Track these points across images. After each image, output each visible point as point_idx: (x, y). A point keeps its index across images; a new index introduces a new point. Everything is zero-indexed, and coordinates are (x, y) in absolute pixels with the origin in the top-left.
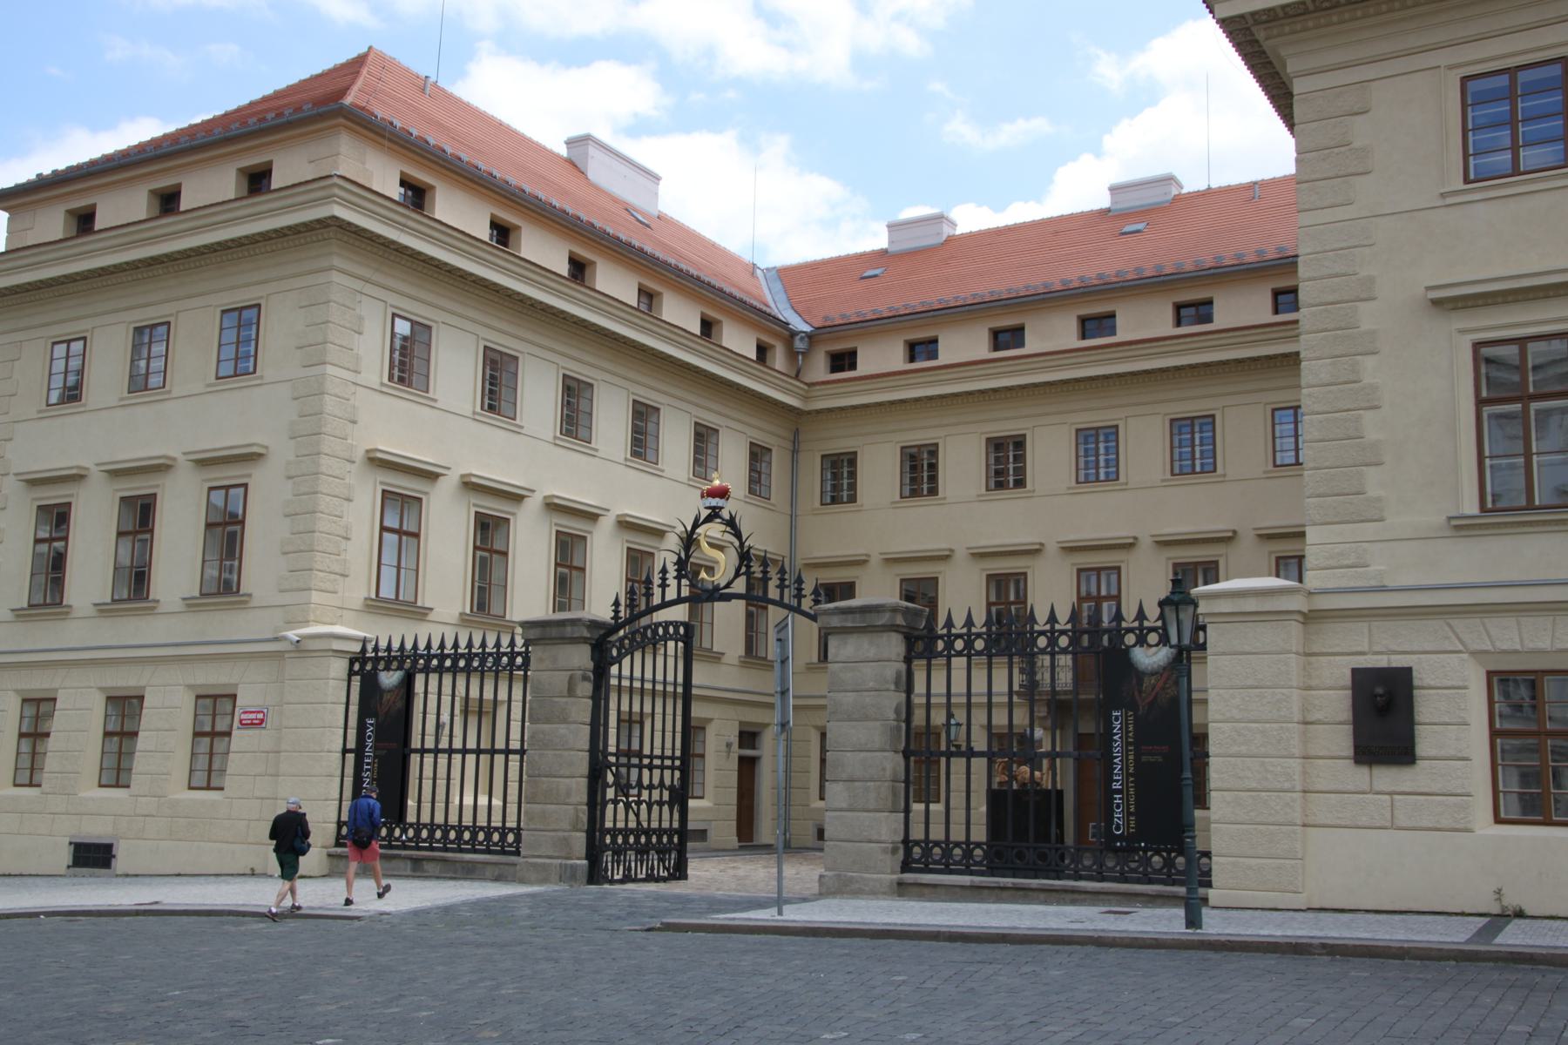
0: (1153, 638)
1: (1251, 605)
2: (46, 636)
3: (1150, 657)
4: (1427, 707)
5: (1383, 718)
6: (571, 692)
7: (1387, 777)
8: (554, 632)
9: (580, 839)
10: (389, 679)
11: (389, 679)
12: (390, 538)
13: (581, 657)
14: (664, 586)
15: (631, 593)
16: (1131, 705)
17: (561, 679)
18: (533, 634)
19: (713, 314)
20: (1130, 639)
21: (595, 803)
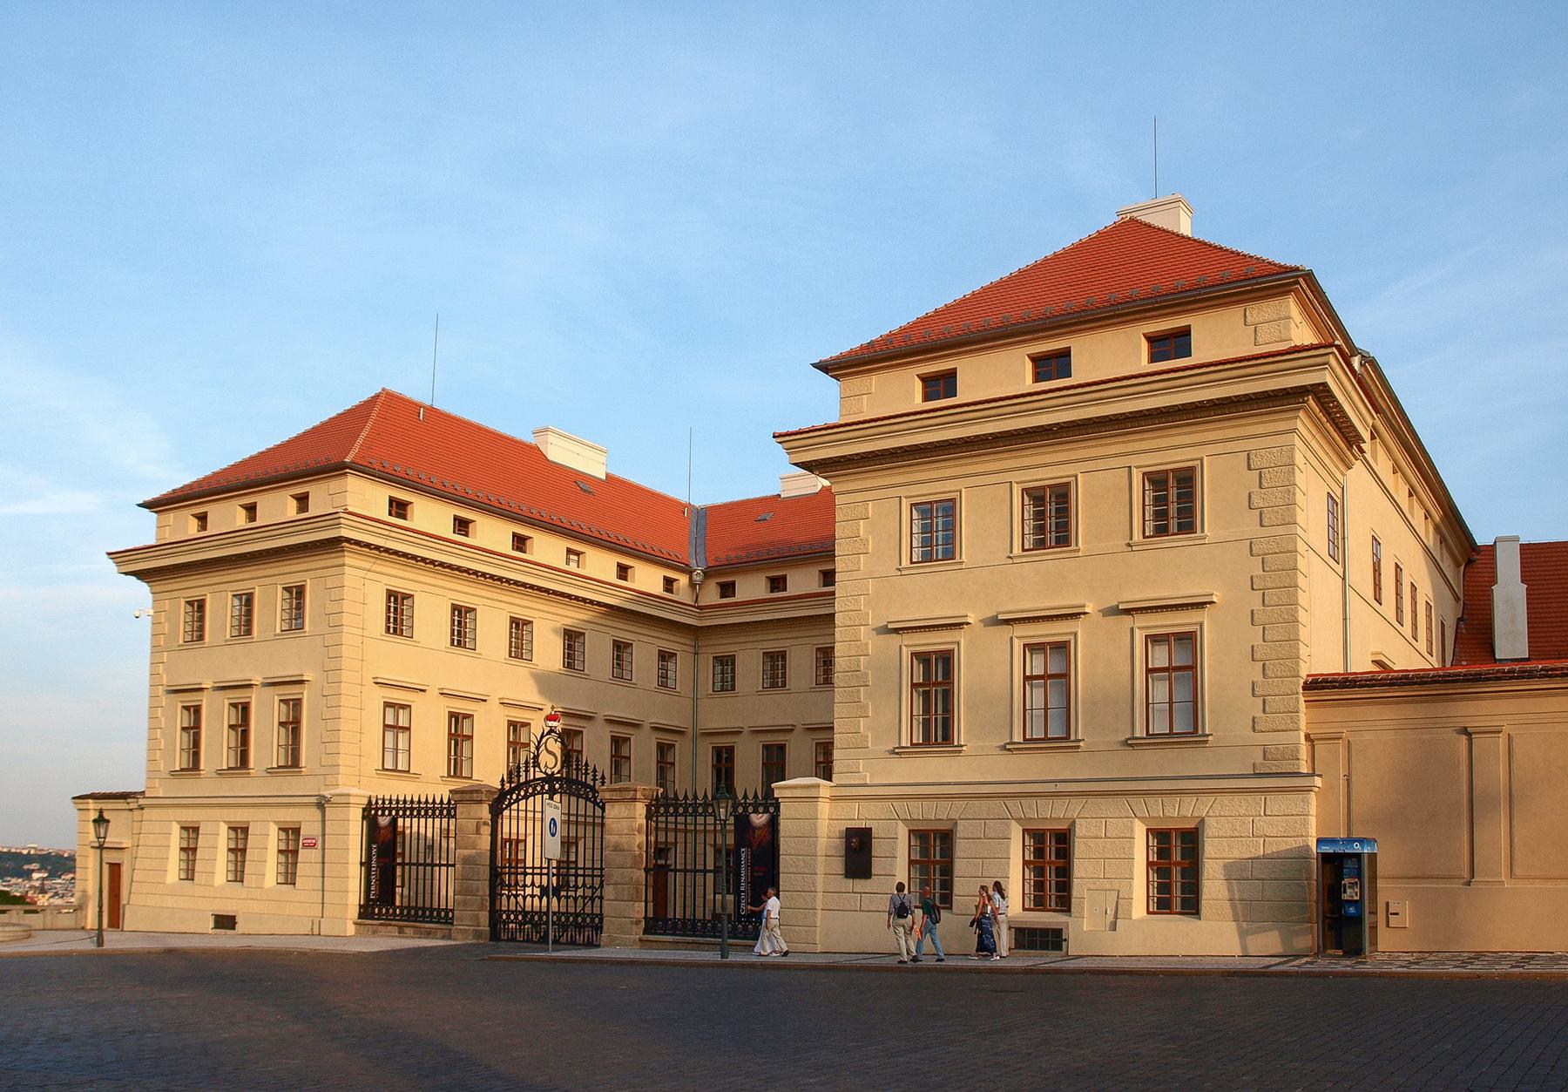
0: (761, 809)
1: (798, 793)
2: (189, 787)
3: (759, 819)
4: (877, 848)
5: (858, 852)
6: (478, 832)
7: (860, 885)
8: (467, 796)
9: (484, 917)
10: (384, 821)
11: (384, 821)
12: (390, 735)
13: (484, 812)
14: (527, 771)
15: (510, 773)
16: (749, 846)
17: (472, 824)
18: (457, 797)
19: (626, 561)
20: (750, 809)
21: (494, 896)
